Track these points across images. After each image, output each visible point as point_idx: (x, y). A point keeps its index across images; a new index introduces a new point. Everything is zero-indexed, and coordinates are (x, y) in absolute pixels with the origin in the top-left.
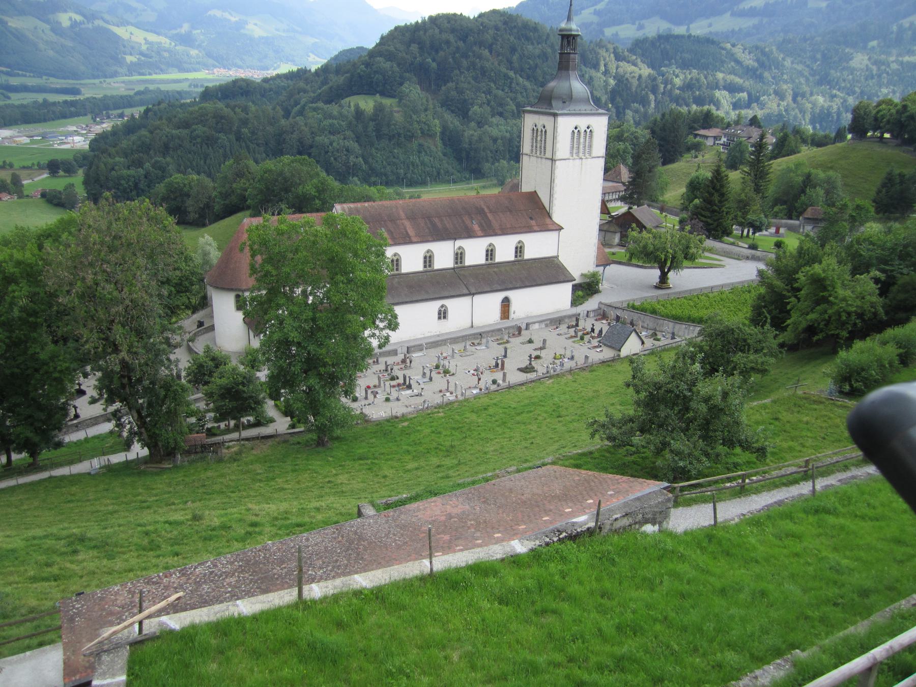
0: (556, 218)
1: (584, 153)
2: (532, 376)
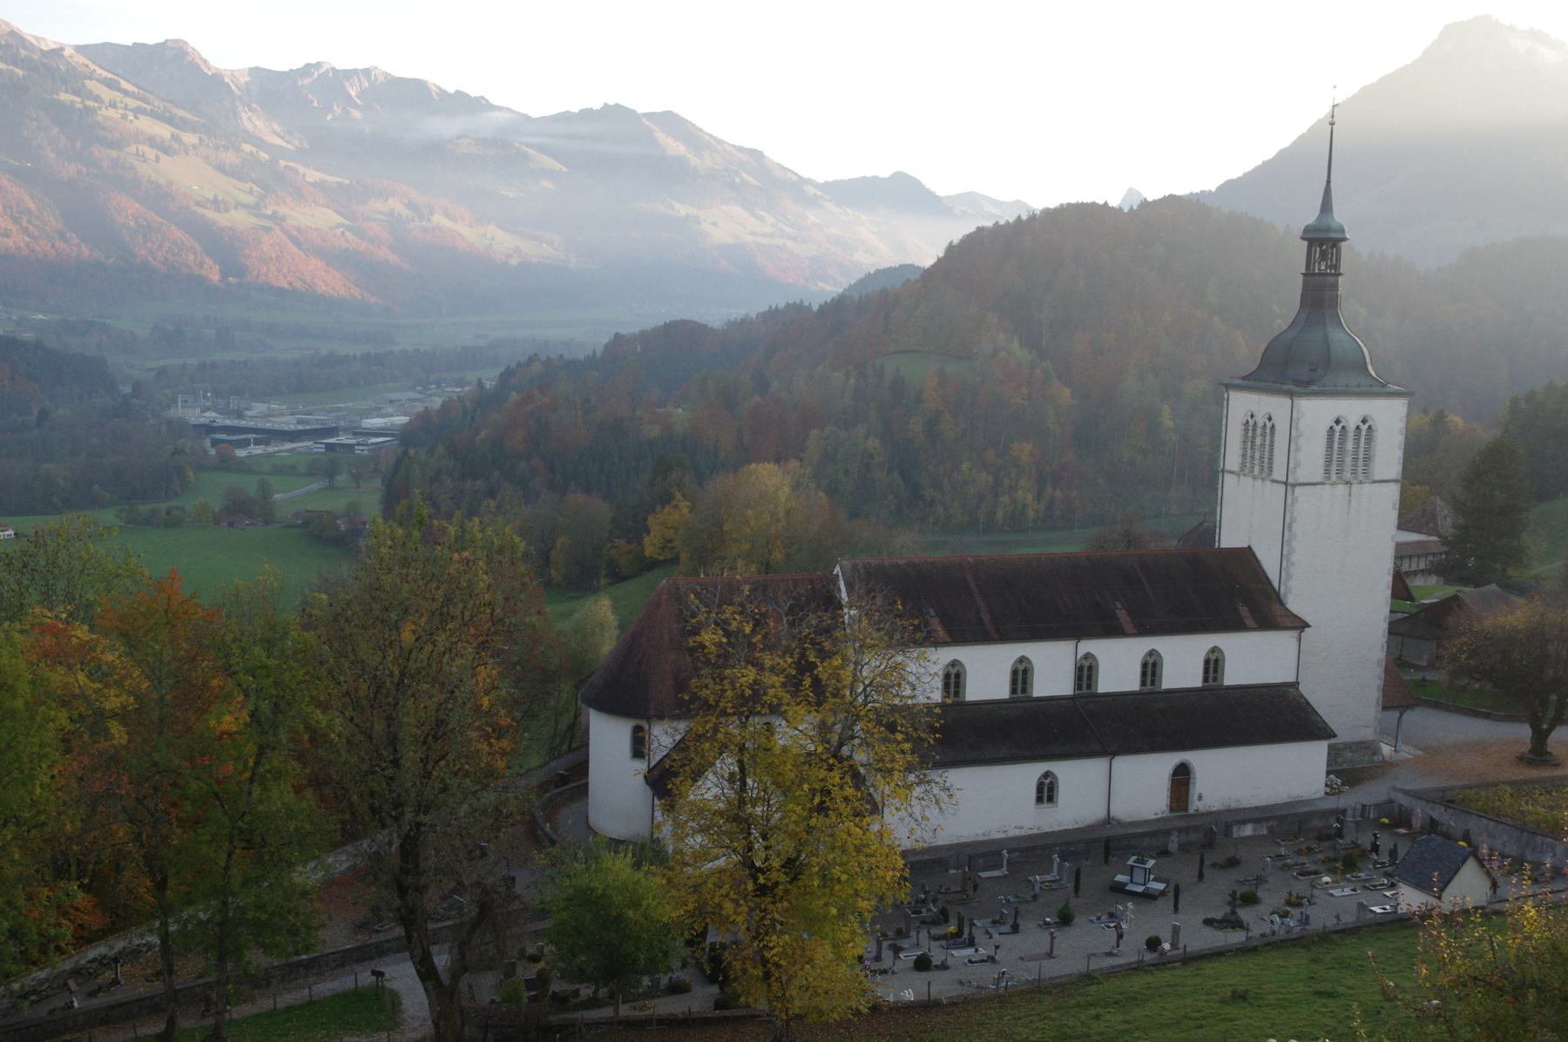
0: (1295, 604)
1: (1354, 472)
2: (1236, 937)
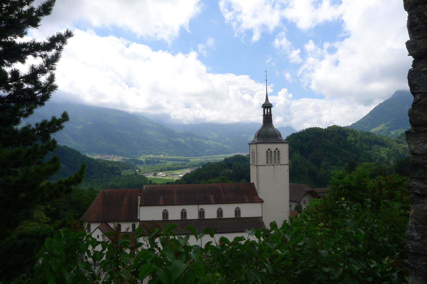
0: (261, 196)
1: (275, 162)
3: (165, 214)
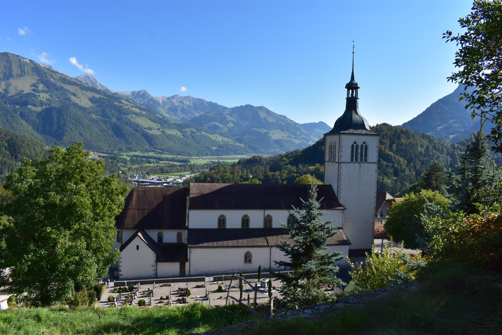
0: (341, 201)
1: (361, 160)
3: (222, 221)
